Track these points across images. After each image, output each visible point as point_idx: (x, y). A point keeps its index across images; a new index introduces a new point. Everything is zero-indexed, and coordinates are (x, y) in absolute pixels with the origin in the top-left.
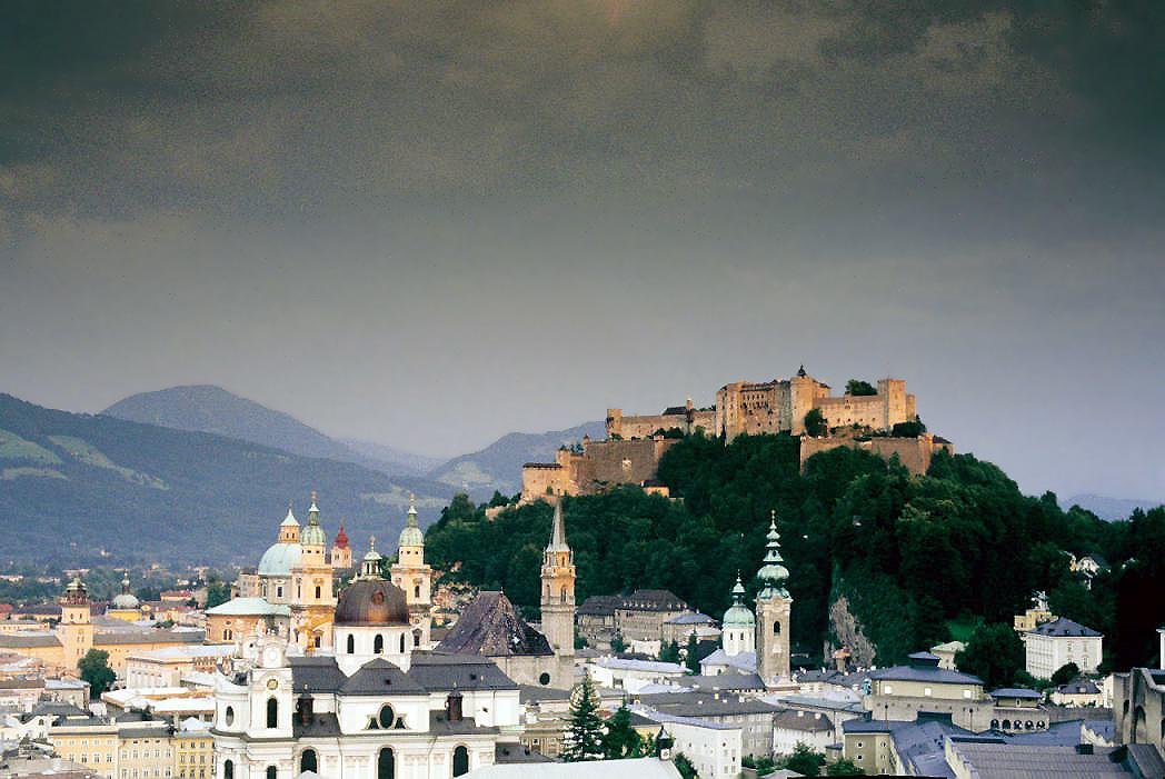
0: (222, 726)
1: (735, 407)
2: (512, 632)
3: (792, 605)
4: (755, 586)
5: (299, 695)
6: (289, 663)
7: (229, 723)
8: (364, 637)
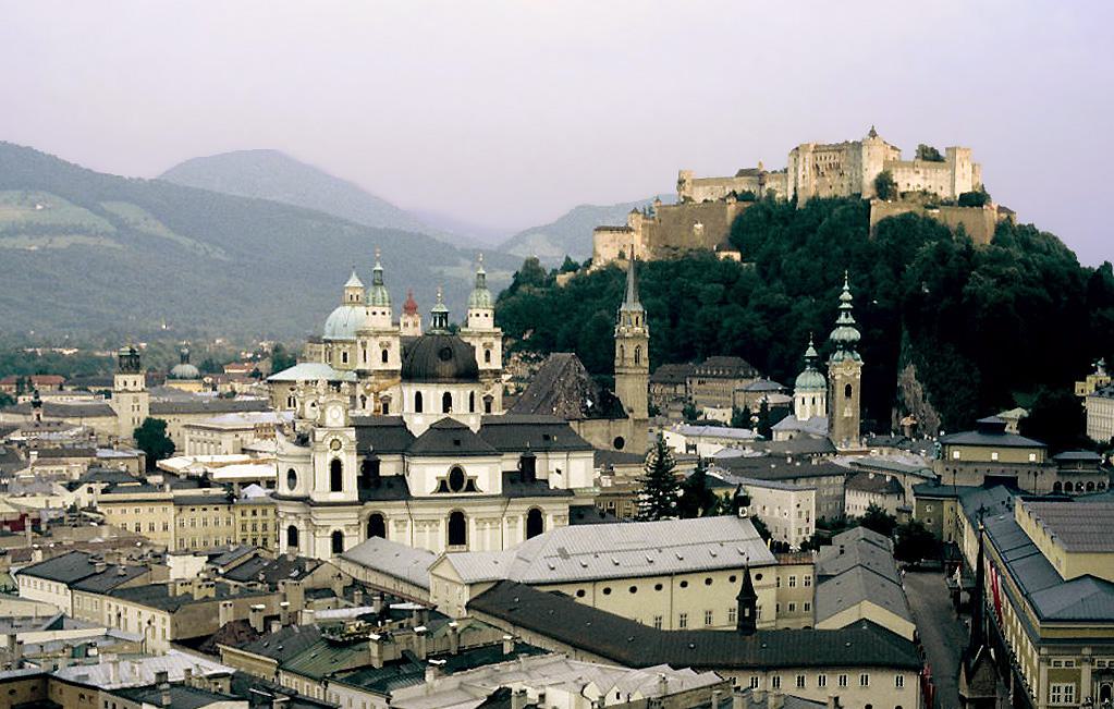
0: (283, 489)
1: (807, 168)
4: (827, 349)
5: (362, 458)
6: (352, 422)
7: (292, 487)
8: (433, 394)
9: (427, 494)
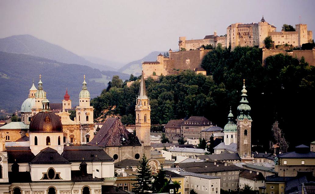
1: (235, 34)
2: (122, 136)
3: (252, 123)
6: (6, 150)
8: (42, 137)
9: (38, 180)
